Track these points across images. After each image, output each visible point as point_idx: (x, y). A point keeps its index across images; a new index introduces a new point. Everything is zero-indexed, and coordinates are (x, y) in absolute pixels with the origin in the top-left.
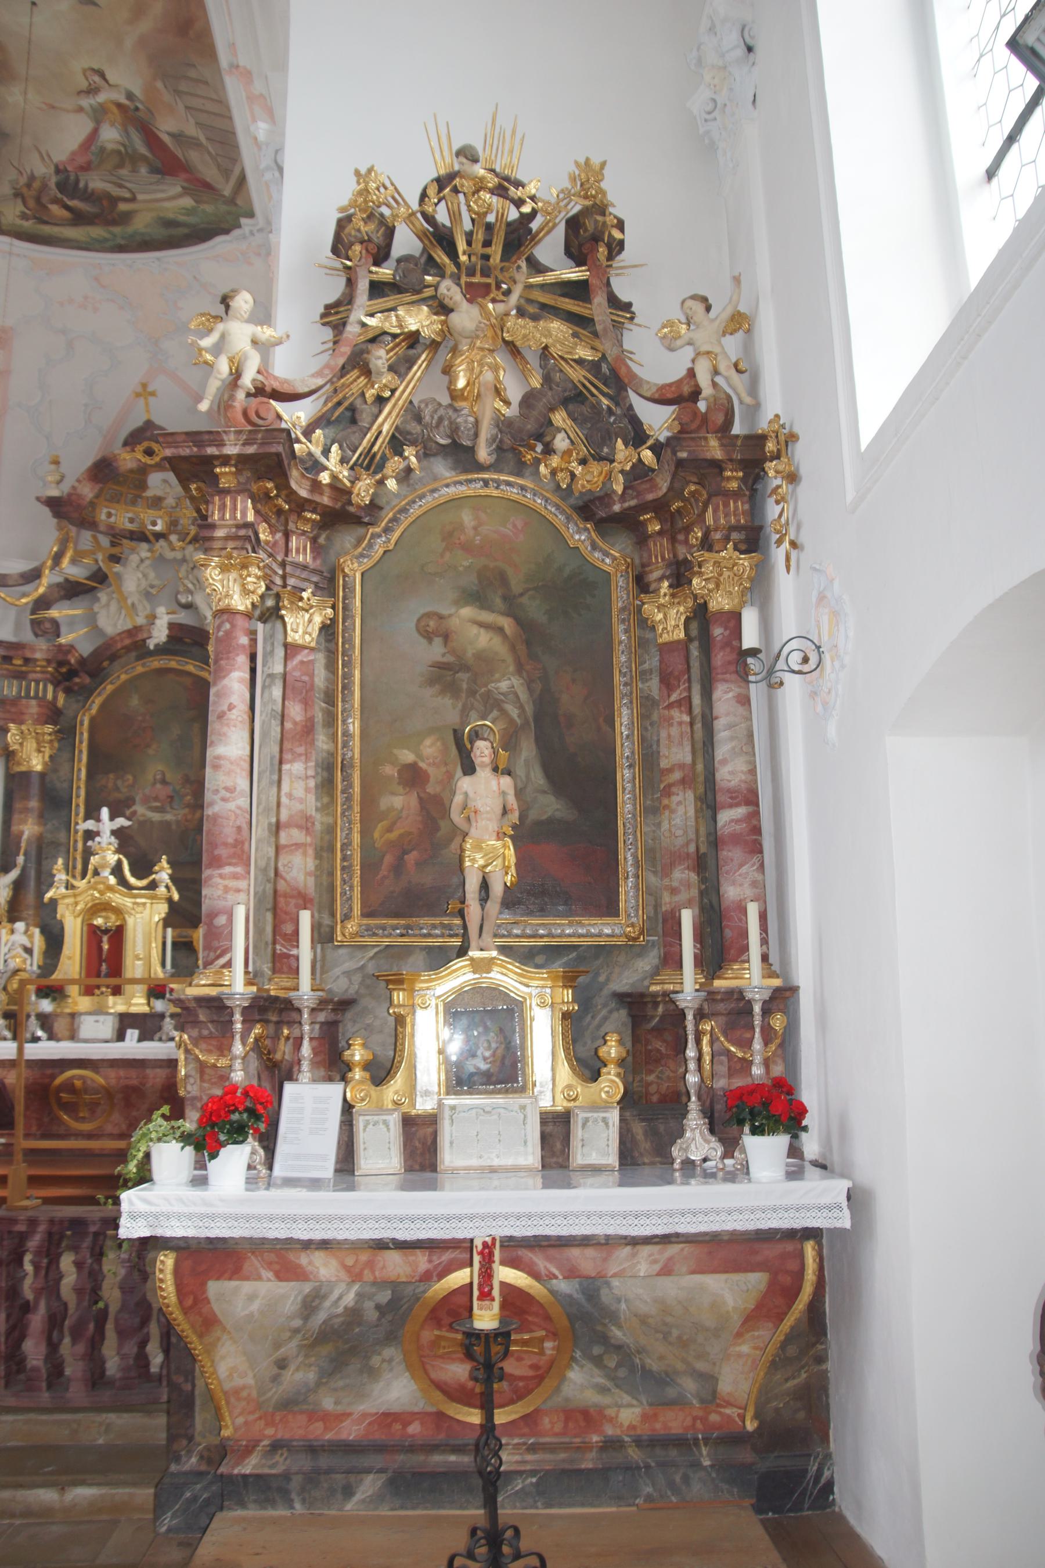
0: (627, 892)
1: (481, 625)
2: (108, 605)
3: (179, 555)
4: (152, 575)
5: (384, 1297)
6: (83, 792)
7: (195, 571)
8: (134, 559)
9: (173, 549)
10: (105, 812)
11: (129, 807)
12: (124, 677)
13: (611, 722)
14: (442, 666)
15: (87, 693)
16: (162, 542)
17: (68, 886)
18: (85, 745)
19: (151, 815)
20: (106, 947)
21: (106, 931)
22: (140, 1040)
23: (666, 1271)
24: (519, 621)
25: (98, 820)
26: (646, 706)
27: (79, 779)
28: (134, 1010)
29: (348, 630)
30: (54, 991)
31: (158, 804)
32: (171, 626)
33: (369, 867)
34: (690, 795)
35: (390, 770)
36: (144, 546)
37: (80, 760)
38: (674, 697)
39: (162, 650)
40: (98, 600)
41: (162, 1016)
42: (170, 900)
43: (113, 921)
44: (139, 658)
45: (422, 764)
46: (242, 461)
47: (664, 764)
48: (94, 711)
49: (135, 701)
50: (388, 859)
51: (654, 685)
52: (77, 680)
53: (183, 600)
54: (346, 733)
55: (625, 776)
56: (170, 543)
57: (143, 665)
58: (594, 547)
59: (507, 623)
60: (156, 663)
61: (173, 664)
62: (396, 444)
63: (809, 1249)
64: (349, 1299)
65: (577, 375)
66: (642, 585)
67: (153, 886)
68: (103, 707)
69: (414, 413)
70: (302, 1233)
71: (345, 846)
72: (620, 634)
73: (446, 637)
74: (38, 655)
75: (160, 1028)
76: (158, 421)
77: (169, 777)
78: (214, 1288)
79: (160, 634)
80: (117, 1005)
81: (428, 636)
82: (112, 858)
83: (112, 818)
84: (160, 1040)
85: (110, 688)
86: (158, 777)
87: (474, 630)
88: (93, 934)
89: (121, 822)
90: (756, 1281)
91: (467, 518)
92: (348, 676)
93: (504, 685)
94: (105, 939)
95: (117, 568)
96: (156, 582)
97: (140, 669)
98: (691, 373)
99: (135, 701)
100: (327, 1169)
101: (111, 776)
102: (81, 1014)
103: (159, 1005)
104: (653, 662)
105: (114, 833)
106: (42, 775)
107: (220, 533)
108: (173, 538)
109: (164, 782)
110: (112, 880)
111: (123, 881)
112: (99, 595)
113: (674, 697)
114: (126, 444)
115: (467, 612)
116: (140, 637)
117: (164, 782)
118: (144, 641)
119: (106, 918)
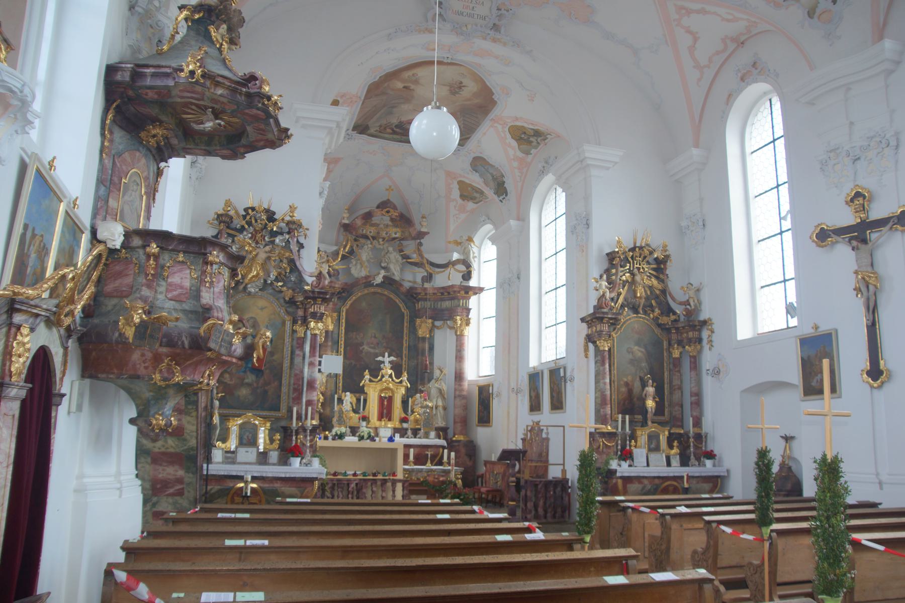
0: (666, 410)
1: (639, 351)
2: (356, 265)
3: (382, 247)
4: (370, 253)
5: (655, 487)
6: (343, 339)
7: (388, 254)
8: (366, 247)
9: (380, 244)
10: (386, 354)
11: (361, 346)
12: (360, 294)
13: (664, 374)
14: (632, 360)
15: (346, 299)
16: (375, 241)
17: (370, 381)
18: (344, 321)
19: (370, 349)
20: (386, 403)
21: (385, 398)
22: (400, 437)
23: (698, 483)
24: (646, 350)
25: (384, 357)
26: (670, 370)
27: (342, 334)
28: (397, 426)
29: (614, 350)
30: (365, 418)
31: (372, 346)
32: (384, 277)
33: (618, 404)
34: (680, 391)
35: (622, 383)
36: (369, 242)
37: (342, 326)
38: (677, 370)
39: (377, 285)
40: (352, 263)
41: (406, 429)
42: (407, 388)
43: (389, 394)
44: (365, 287)
45: (628, 382)
46: (611, 319)
47: (674, 384)
48: (347, 307)
49: (364, 304)
50: (622, 402)
51: (671, 366)
52: (343, 294)
53: (383, 265)
54: (614, 374)
55: (666, 386)
56: (379, 242)
57: (368, 290)
58: (661, 334)
59: (643, 350)
60: (372, 290)
61: (379, 291)
62: (622, 306)
63: (719, 480)
64: (649, 487)
65: (658, 292)
66: (670, 344)
67: (401, 382)
68: (351, 304)
69: (625, 299)
70: (646, 475)
71: (614, 399)
72: (665, 354)
73: (632, 353)
74: (337, 286)
75: (406, 433)
76: (391, 200)
77: (377, 336)
78: (628, 486)
79: (379, 280)
80: (390, 425)
81: (629, 352)
82: (390, 372)
83: (389, 357)
84: (408, 437)
85: (354, 298)
86: (373, 335)
87: (638, 352)
88: (381, 399)
89: (392, 358)
90: (711, 485)
91: (636, 326)
92: (614, 361)
93: (643, 365)
94: (386, 400)
95: (360, 251)
96: (372, 257)
97: (366, 292)
98: (688, 300)
99: (364, 304)
100: (646, 465)
101: (355, 333)
102: (379, 428)
103: (405, 425)
104: (671, 361)
105: (389, 362)
106: (332, 332)
107: (604, 333)
108: (381, 240)
109: (375, 337)
110: (391, 380)
111: (393, 380)
112: (352, 261)
113: (677, 370)
114: (378, 207)
115: (636, 348)
116: (369, 280)
117: (375, 337)
118: (371, 281)
119: (386, 393)
